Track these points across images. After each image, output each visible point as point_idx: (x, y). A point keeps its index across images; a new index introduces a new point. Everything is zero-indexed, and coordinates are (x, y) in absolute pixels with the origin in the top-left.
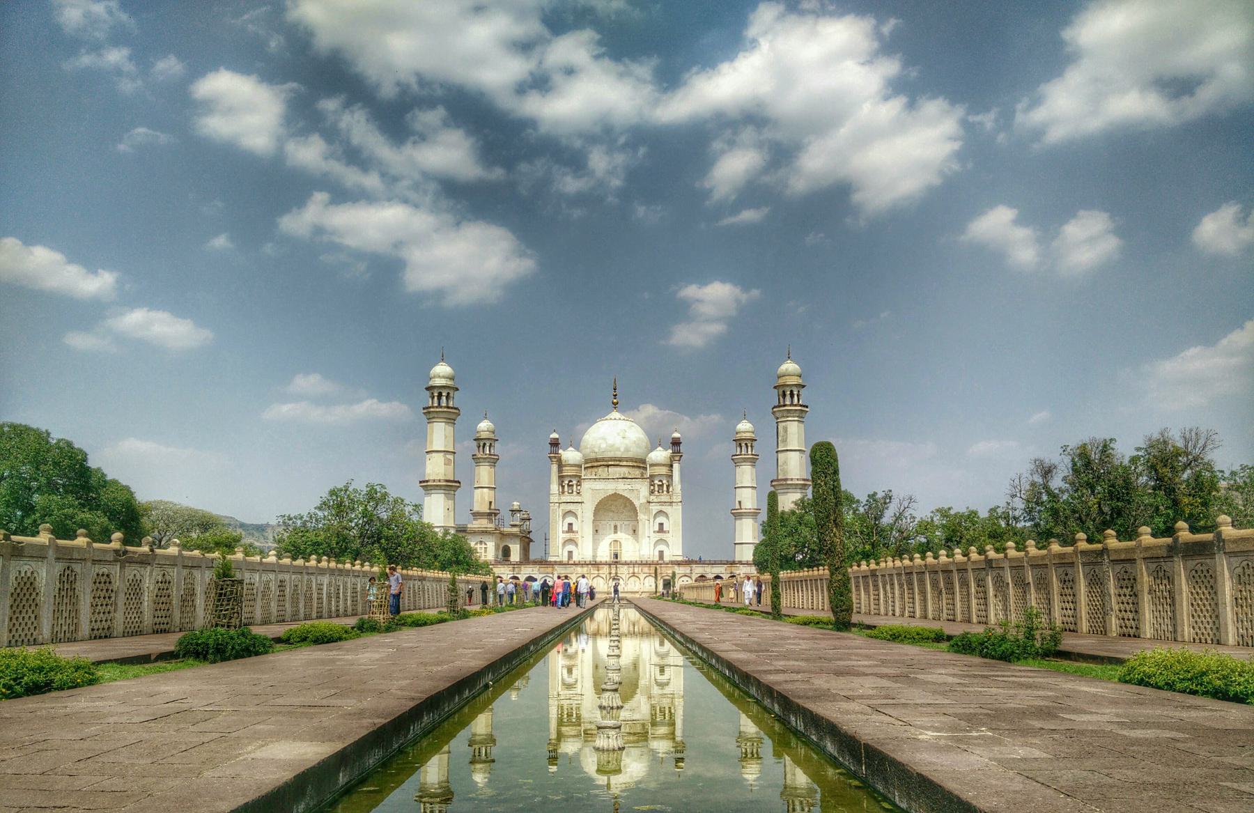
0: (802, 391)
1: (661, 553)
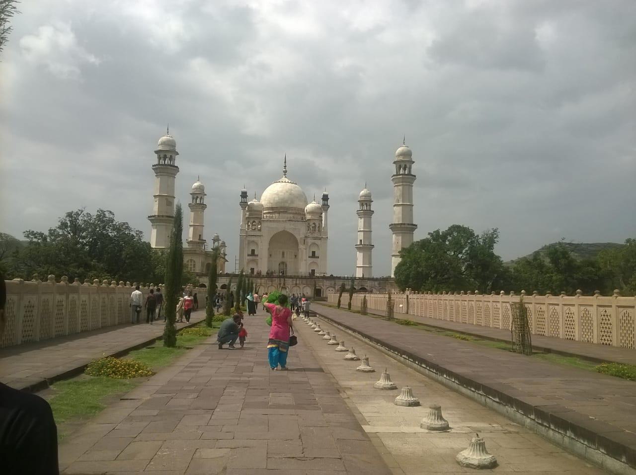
0: (413, 166)
1: (313, 271)
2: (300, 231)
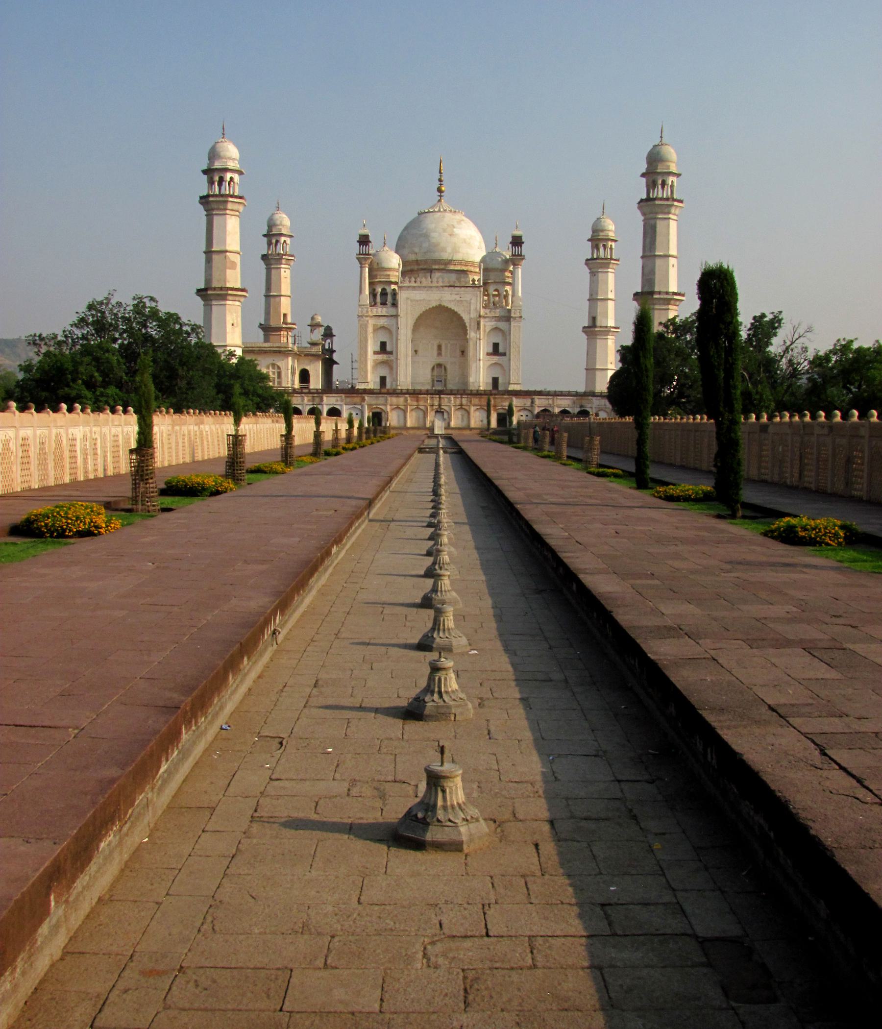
2: (469, 304)
